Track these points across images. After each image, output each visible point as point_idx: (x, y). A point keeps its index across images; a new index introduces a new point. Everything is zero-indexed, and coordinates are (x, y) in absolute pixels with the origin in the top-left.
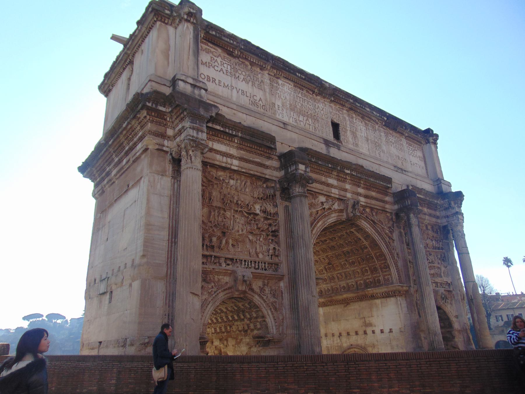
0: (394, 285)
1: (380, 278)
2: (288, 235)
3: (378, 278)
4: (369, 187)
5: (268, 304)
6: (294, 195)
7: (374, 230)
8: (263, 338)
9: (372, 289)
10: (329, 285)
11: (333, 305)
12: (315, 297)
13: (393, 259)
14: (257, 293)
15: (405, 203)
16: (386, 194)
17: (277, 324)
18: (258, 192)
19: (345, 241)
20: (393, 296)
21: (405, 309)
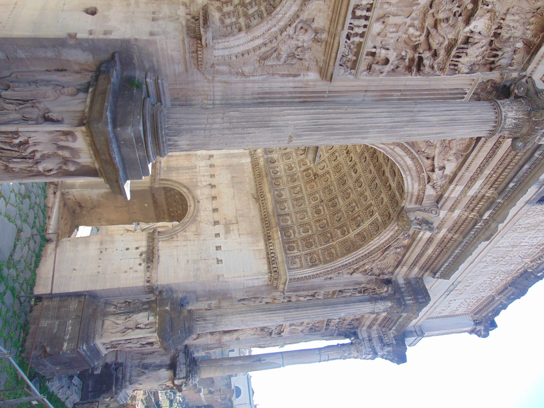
0: (287, 271)
1: (295, 251)
2: (406, 95)
3: (296, 248)
4: (444, 245)
5: (276, 38)
6: (502, 108)
7: (374, 249)
8: (204, 24)
9: (280, 239)
10: (283, 173)
11: (255, 178)
12: (290, 141)
13: (325, 272)
14: (301, 10)
15: (408, 296)
16: (421, 269)
17: (234, 58)
18: (515, 25)
19: (355, 202)
20: (269, 268)
21: (250, 284)
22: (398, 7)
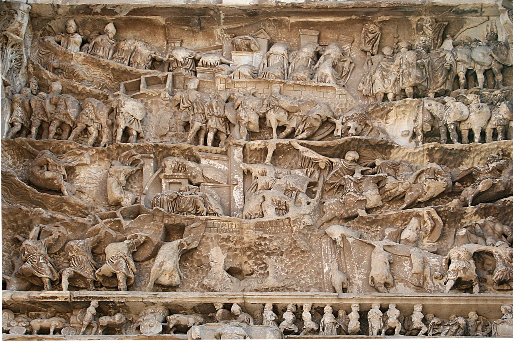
18: (393, 69)
22: (353, 269)
